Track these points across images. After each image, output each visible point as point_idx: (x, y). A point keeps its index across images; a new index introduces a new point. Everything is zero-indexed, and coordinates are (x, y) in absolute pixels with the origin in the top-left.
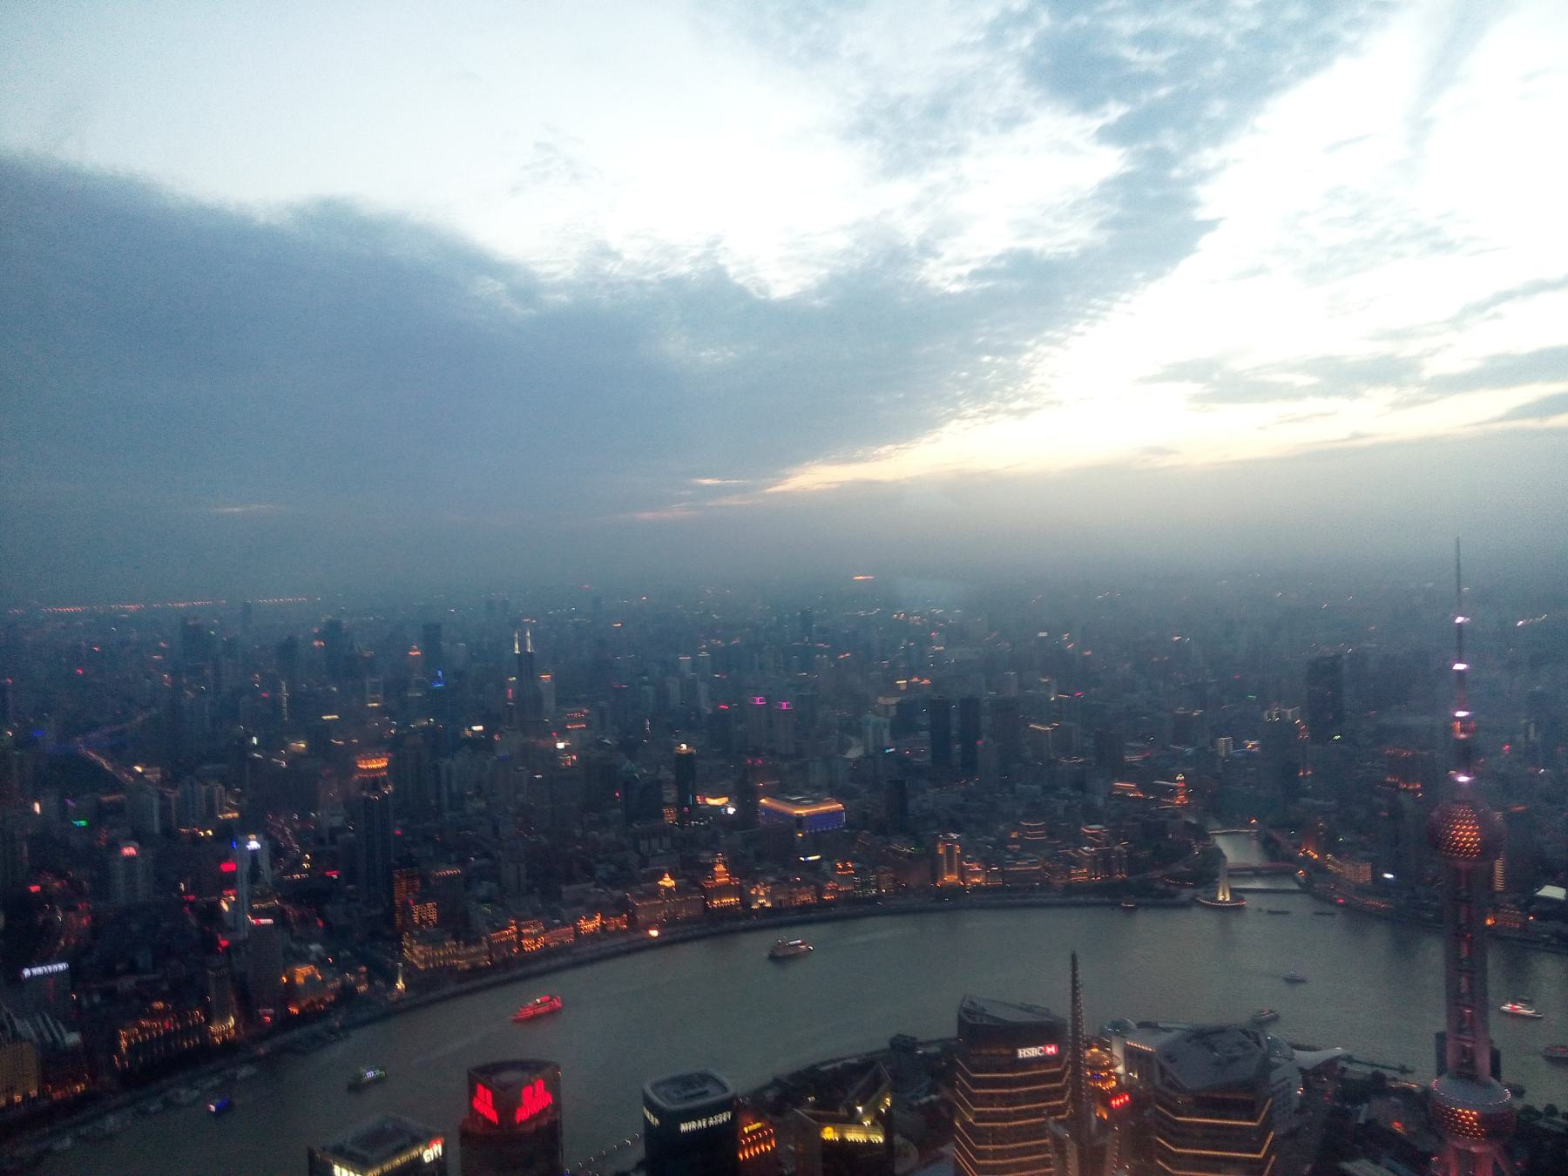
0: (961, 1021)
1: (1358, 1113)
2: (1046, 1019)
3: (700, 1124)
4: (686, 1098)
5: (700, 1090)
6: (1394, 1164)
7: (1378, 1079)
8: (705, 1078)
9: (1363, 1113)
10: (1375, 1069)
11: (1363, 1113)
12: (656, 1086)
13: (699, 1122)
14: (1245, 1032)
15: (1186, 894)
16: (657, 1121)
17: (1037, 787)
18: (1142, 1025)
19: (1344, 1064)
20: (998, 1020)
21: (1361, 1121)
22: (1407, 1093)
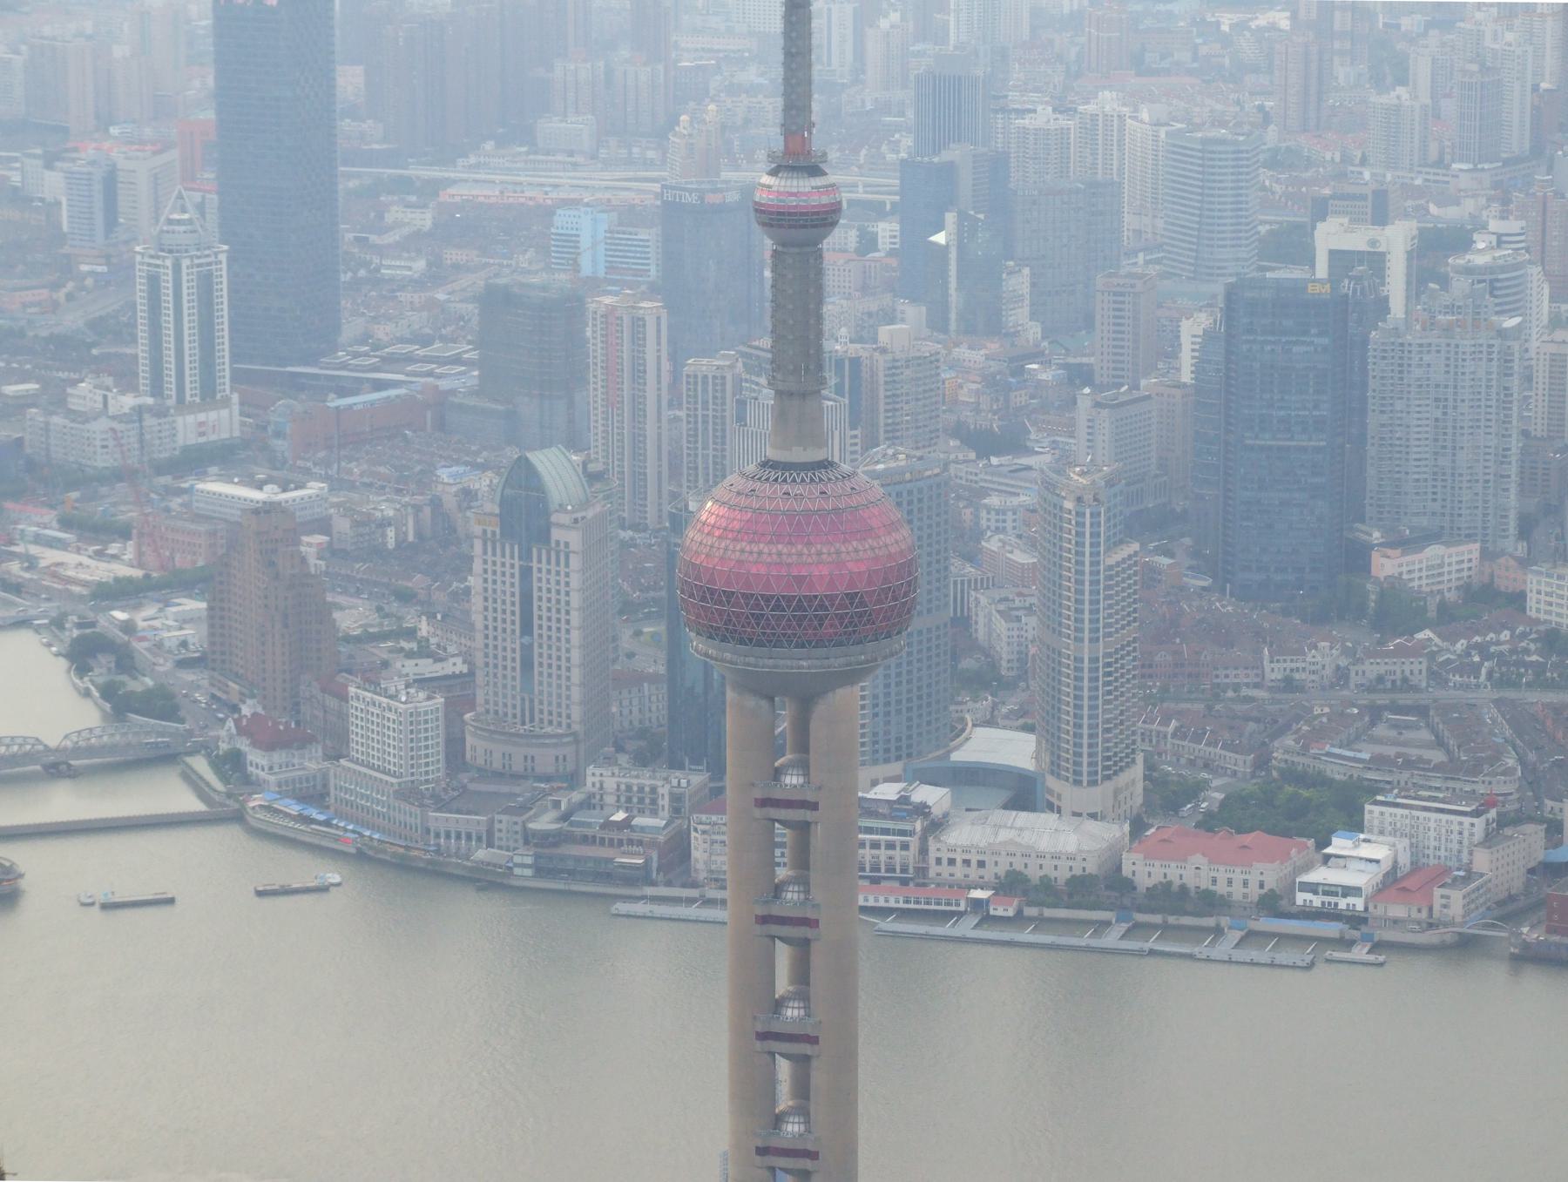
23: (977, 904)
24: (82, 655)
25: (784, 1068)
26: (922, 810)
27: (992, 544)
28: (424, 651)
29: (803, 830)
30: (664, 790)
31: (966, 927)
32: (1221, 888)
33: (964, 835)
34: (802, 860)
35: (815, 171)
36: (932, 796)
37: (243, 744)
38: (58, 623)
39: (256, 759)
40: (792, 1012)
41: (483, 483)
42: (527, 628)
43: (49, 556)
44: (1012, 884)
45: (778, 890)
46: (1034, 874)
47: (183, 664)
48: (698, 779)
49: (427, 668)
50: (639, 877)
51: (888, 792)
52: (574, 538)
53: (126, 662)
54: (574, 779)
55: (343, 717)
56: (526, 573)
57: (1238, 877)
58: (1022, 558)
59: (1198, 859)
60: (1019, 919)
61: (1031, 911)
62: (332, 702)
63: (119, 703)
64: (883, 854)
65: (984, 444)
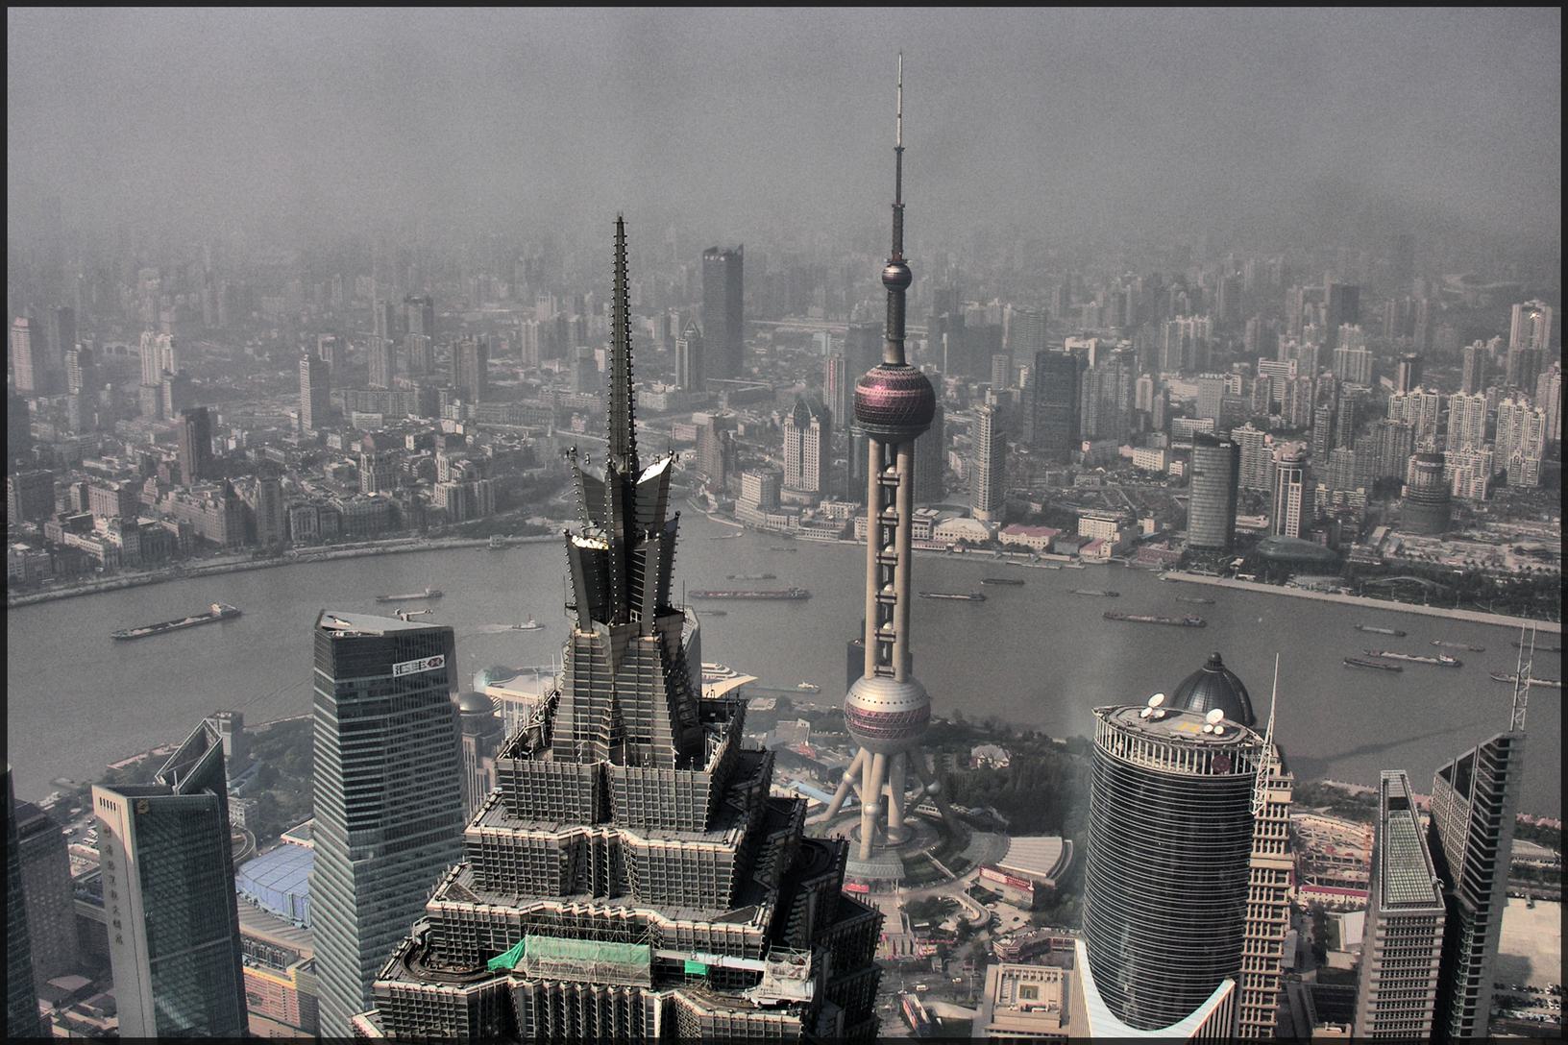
17: (378, 416)
22: (812, 717)
23: (949, 548)
30: (846, 509)
32: (1031, 545)
37: (707, 493)
39: (711, 497)
42: (802, 461)
46: (969, 539)
48: (858, 505)
54: (817, 506)
55: (740, 484)
56: (802, 438)
57: (1036, 540)
59: (1024, 535)
61: (967, 551)
62: (736, 480)
64: (918, 531)
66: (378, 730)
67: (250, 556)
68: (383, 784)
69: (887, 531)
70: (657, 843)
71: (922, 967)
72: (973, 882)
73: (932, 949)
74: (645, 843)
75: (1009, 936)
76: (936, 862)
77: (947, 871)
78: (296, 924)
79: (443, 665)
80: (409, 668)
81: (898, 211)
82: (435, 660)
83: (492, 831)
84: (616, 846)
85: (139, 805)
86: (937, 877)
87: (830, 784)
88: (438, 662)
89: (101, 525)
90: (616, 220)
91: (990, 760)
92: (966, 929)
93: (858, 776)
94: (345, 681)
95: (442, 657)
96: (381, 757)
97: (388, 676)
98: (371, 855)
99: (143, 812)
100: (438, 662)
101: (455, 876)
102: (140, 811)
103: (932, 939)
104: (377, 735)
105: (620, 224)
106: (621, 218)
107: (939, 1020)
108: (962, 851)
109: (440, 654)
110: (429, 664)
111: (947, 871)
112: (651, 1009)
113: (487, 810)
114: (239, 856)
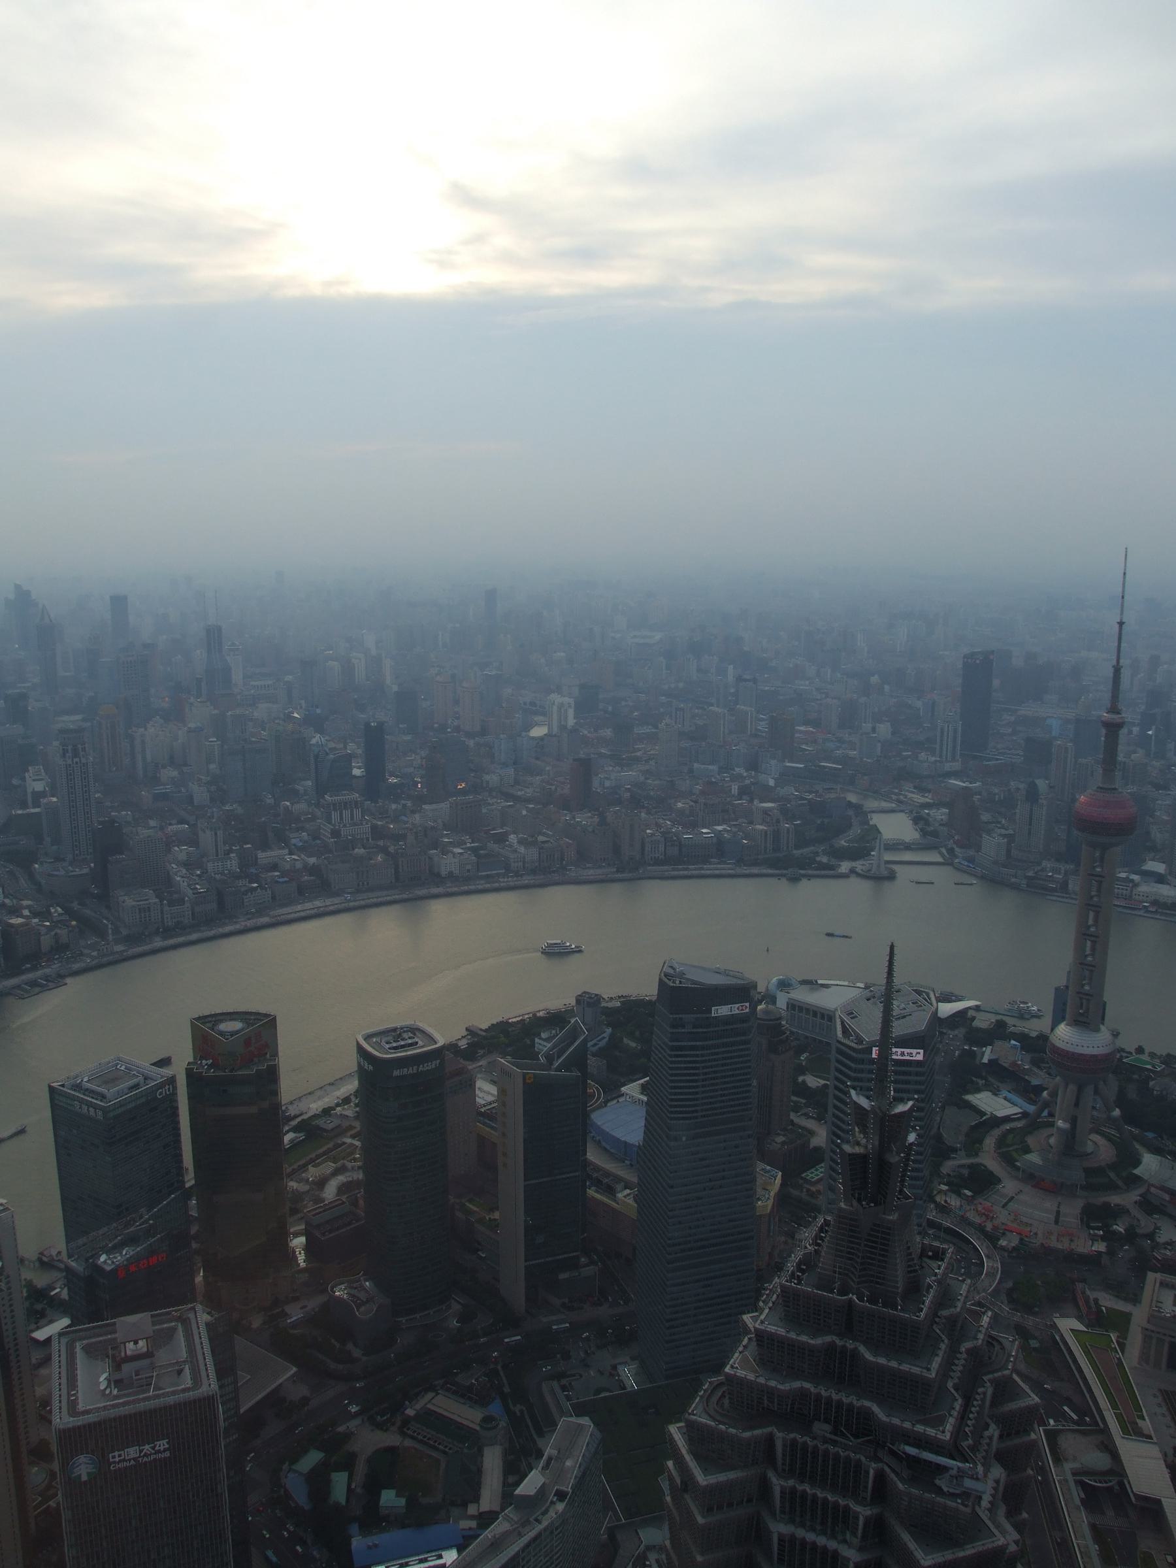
0: (660, 980)
1: (983, 1054)
2: (740, 982)
3: (411, 1071)
4: (395, 1048)
5: (410, 1041)
6: (1010, 1096)
7: (1001, 1025)
8: (414, 1030)
9: (987, 1054)
10: (999, 1017)
11: (987, 1054)
12: (368, 1038)
13: (411, 1068)
14: (919, 992)
15: (845, 867)
16: (371, 1068)
18: (805, 982)
19: (971, 1013)
20: (703, 984)
21: (985, 1060)
22: (1023, 1038)
24: (917, 820)
25: (1089, 944)
26: (1132, 881)
27: (1158, 814)
28: (1003, 827)
29: (1100, 883)
30: (1063, 868)
31: (1141, 913)
33: (1144, 888)
34: (1099, 891)
35: (1119, 713)
36: (1136, 877)
37: (955, 846)
38: (911, 812)
39: (958, 850)
40: (1092, 929)
41: (1022, 786)
42: (1030, 824)
43: (911, 795)
44: (1155, 903)
45: (1092, 897)
47: (940, 825)
49: (1003, 831)
50: (1054, 890)
51: (1123, 875)
52: (1045, 802)
53: (927, 823)
56: (1031, 810)
58: (1165, 818)
60: (1156, 912)
61: (1160, 910)
63: (924, 833)
64: (1120, 891)
65: (1158, 787)
66: (698, 1053)
67: (615, 870)
68: (697, 1090)
69: (1091, 915)
70: (882, 1361)
71: (1092, 1261)
72: (1140, 1196)
73: (1101, 1247)
74: (871, 1358)
75: (1169, 1247)
76: (1112, 1175)
77: (1120, 1183)
78: (626, 1162)
79: (747, 1010)
80: (723, 1011)
81: (1117, 670)
82: (742, 1006)
83: (772, 1329)
84: (855, 1354)
85: (527, 1077)
86: (1112, 1187)
87: (1032, 1096)
88: (744, 1008)
89: (513, 838)
90: (890, 944)
91: (1164, 1093)
92: (1131, 1236)
93: (1054, 1094)
94: (677, 1016)
95: (747, 1004)
96: (697, 1071)
97: (707, 1016)
98: (684, 1139)
99: (529, 1082)
100: (744, 1008)
101: (745, 1347)
102: (528, 1081)
103: (1103, 1238)
104: (697, 1056)
105: (892, 947)
106: (892, 943)
107: (1104, 1308)
108: (1135, 1168)
109: (746, 1002)
110: (738, 1009)
111: (1120, 1183)
112: (867, 1472)
113: (770, 1308)
114: (591, 1105)
